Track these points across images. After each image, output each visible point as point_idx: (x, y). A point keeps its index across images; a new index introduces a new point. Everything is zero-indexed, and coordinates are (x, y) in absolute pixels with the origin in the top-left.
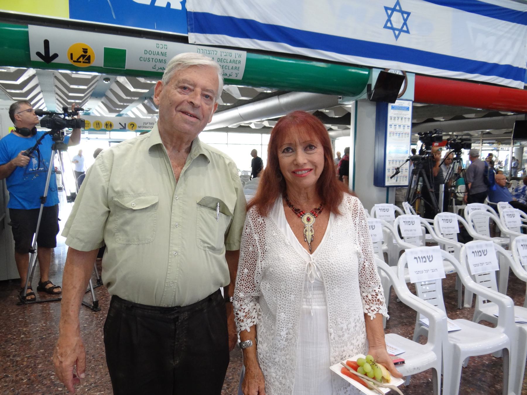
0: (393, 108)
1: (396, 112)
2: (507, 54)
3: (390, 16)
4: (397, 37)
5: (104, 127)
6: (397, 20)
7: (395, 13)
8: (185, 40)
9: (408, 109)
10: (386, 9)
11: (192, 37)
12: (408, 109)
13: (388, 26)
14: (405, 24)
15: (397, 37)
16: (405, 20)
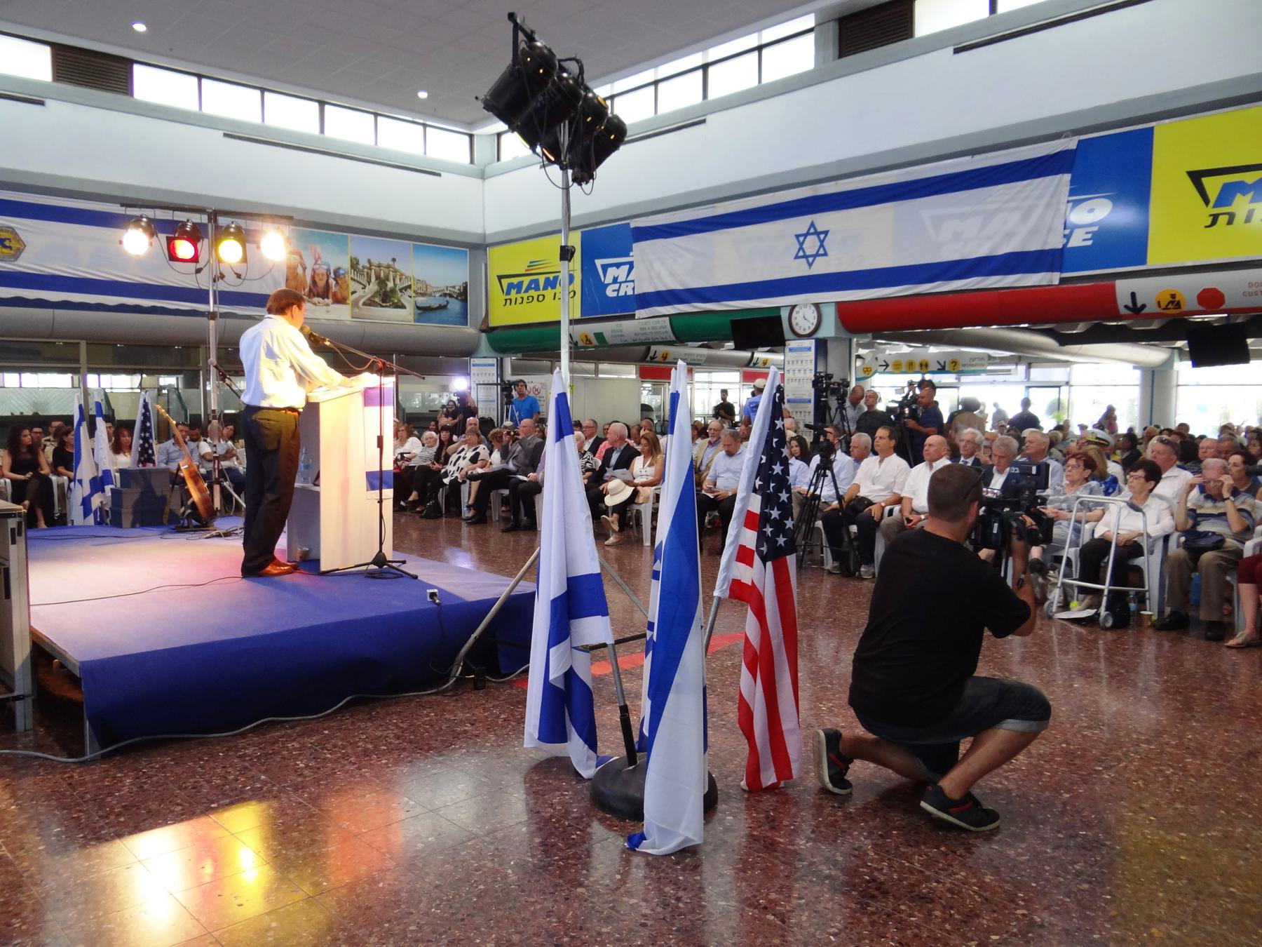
0: (791, 350)
1: (795, 354)
2: (1010, 235)
3: (801, 244)
4: (810, 265)
5: (918, 368)
6: (811, 245)
7: (809, 237)
8: (632, 317)
9: (809, 349)
10: (797, 236)
11: (640, 313)
12: (809, 349)
13: (801, 255)
14: (822, 245)
15: (810, 265)
16: (822, 242)
